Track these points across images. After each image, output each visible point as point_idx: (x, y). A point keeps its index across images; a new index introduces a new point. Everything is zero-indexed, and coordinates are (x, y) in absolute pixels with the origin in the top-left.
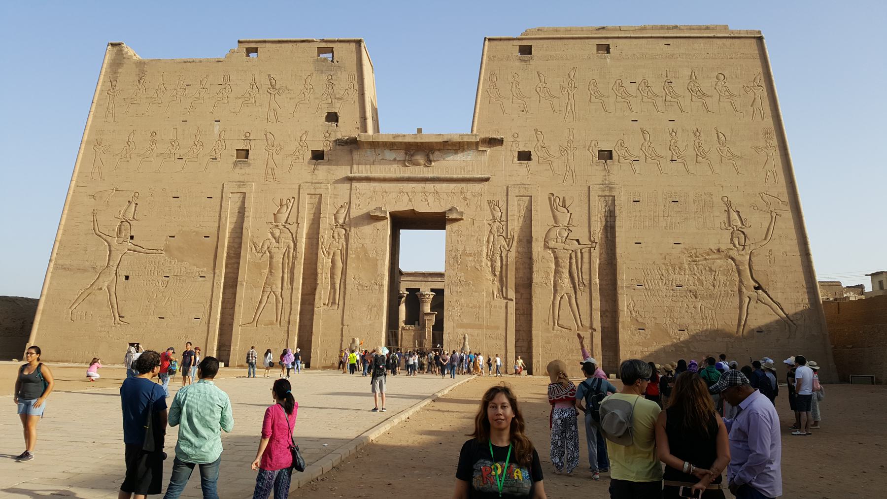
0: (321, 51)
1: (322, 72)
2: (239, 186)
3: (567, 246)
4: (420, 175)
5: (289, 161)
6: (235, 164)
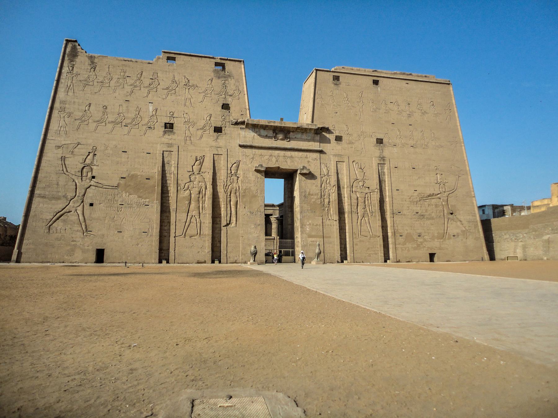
0: (217, 64)
1: (219, 78)
2: (168, 147)
4: (283, 146)
5: (200, 132)
6: (165, 132)
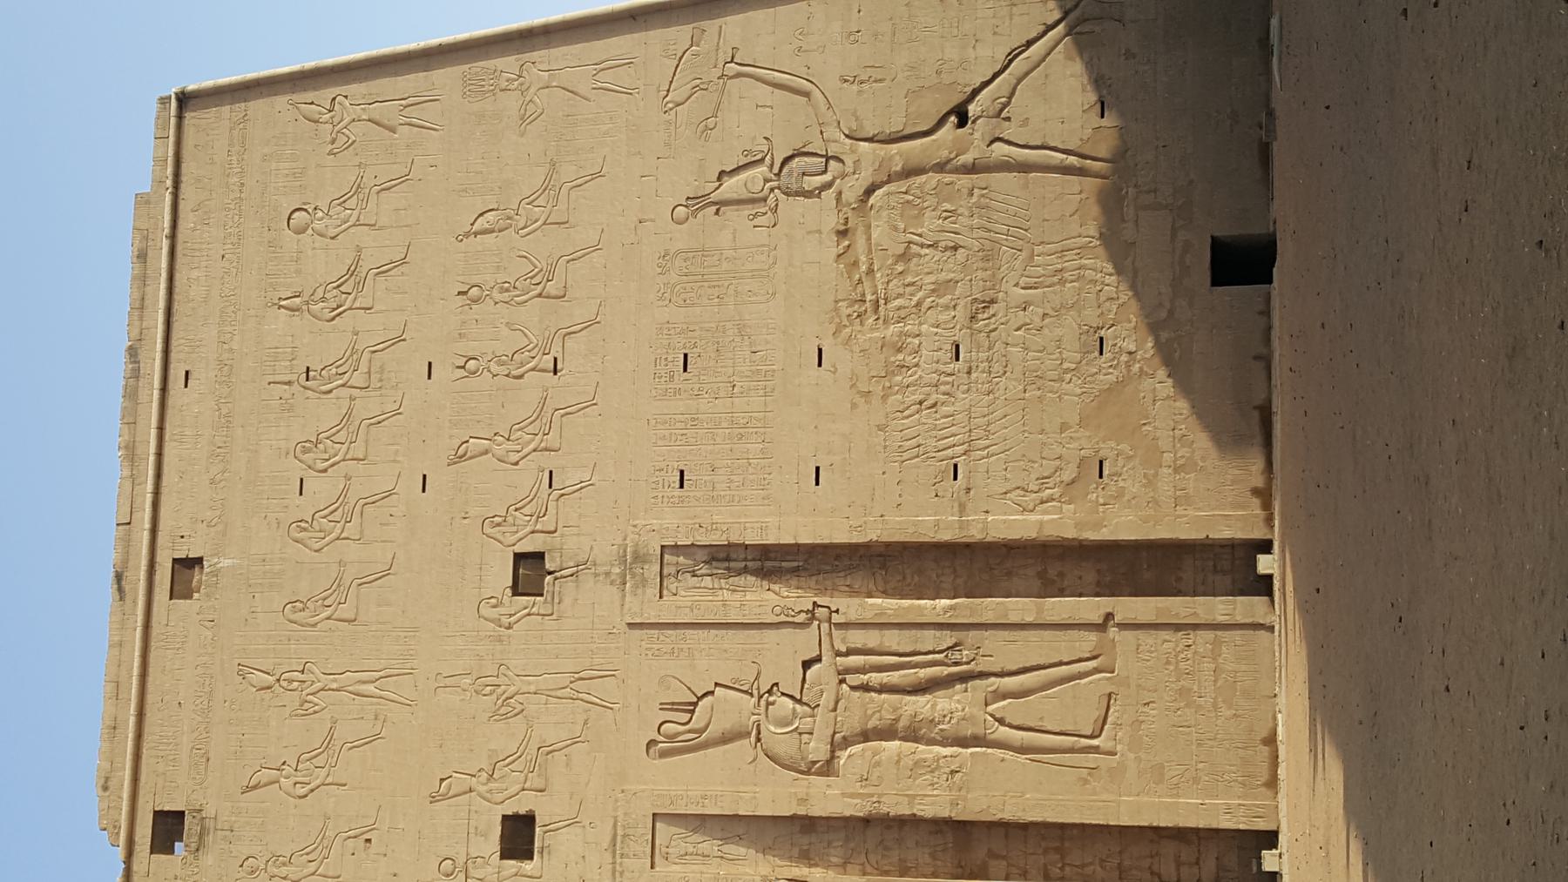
3: (826, 700)
